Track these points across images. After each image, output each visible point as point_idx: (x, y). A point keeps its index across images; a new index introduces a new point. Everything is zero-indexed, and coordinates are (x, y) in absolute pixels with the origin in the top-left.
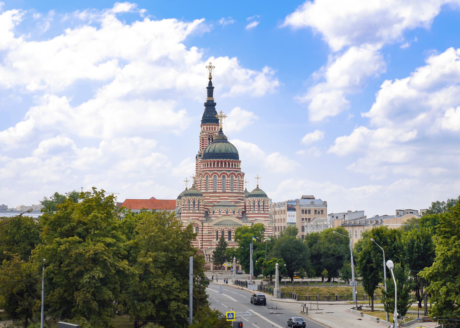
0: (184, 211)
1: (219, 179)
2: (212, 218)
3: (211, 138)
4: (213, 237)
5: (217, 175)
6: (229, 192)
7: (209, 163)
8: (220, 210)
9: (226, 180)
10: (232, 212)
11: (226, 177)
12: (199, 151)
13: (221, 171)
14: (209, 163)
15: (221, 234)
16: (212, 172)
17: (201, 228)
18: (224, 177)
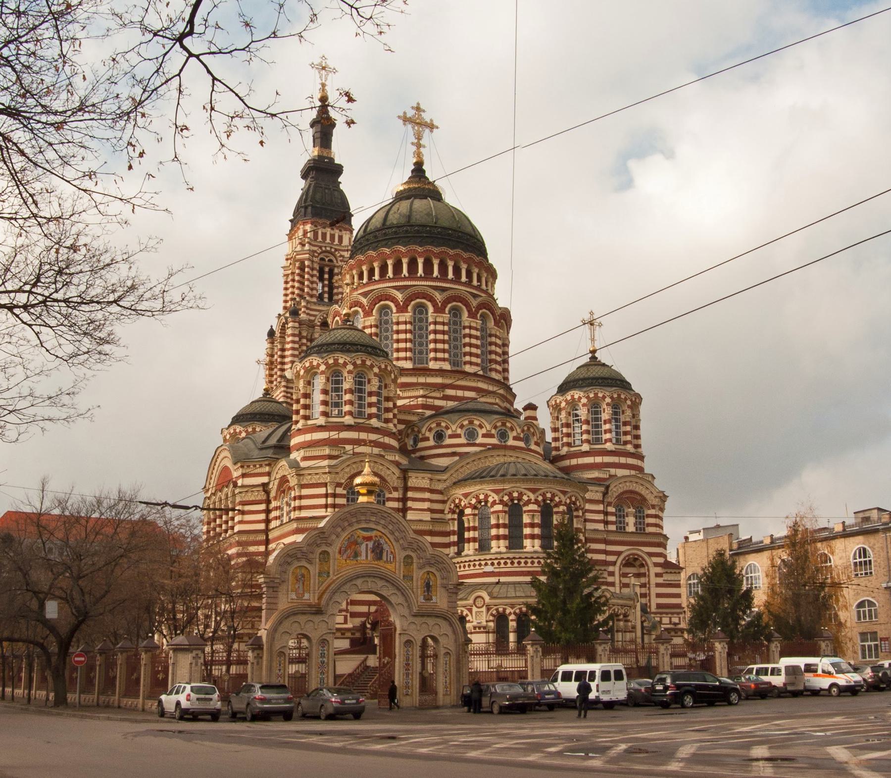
0: (310, 422)
1: (439, 320)
2: (435, 462)
3: (327, 266)
4: (454, 538)
5: (429, 304)
6: (475, 375)
7: (390, 262)
8: (471, 422)
9: (465, 328)
10: (522, 436)
11: (465, 314)
12: (282, 312)
13: (443, 290)
14: (390, 262)
15: (504, 519)
16: (409, 291)
17: (395, 495)
18: (456, 312)
